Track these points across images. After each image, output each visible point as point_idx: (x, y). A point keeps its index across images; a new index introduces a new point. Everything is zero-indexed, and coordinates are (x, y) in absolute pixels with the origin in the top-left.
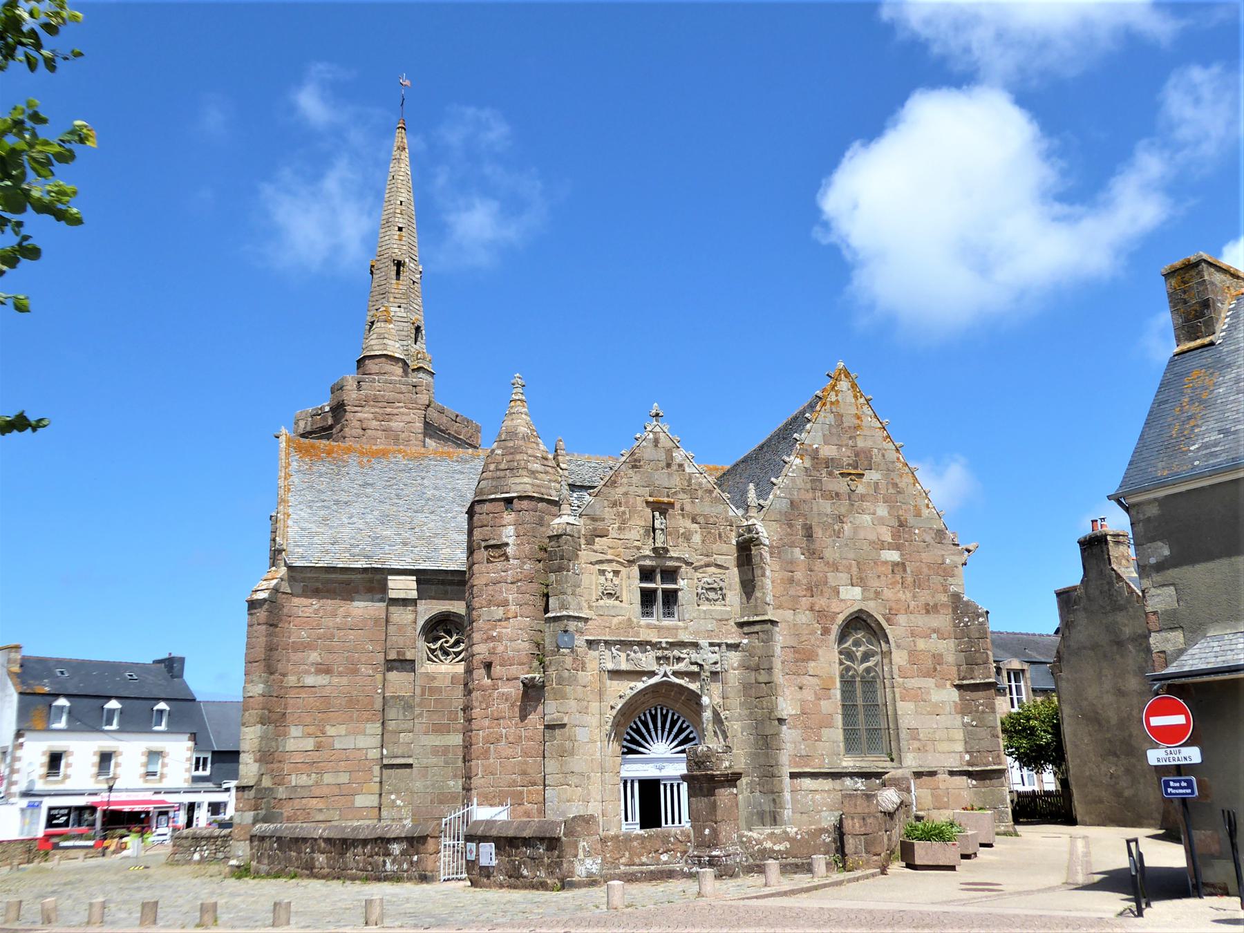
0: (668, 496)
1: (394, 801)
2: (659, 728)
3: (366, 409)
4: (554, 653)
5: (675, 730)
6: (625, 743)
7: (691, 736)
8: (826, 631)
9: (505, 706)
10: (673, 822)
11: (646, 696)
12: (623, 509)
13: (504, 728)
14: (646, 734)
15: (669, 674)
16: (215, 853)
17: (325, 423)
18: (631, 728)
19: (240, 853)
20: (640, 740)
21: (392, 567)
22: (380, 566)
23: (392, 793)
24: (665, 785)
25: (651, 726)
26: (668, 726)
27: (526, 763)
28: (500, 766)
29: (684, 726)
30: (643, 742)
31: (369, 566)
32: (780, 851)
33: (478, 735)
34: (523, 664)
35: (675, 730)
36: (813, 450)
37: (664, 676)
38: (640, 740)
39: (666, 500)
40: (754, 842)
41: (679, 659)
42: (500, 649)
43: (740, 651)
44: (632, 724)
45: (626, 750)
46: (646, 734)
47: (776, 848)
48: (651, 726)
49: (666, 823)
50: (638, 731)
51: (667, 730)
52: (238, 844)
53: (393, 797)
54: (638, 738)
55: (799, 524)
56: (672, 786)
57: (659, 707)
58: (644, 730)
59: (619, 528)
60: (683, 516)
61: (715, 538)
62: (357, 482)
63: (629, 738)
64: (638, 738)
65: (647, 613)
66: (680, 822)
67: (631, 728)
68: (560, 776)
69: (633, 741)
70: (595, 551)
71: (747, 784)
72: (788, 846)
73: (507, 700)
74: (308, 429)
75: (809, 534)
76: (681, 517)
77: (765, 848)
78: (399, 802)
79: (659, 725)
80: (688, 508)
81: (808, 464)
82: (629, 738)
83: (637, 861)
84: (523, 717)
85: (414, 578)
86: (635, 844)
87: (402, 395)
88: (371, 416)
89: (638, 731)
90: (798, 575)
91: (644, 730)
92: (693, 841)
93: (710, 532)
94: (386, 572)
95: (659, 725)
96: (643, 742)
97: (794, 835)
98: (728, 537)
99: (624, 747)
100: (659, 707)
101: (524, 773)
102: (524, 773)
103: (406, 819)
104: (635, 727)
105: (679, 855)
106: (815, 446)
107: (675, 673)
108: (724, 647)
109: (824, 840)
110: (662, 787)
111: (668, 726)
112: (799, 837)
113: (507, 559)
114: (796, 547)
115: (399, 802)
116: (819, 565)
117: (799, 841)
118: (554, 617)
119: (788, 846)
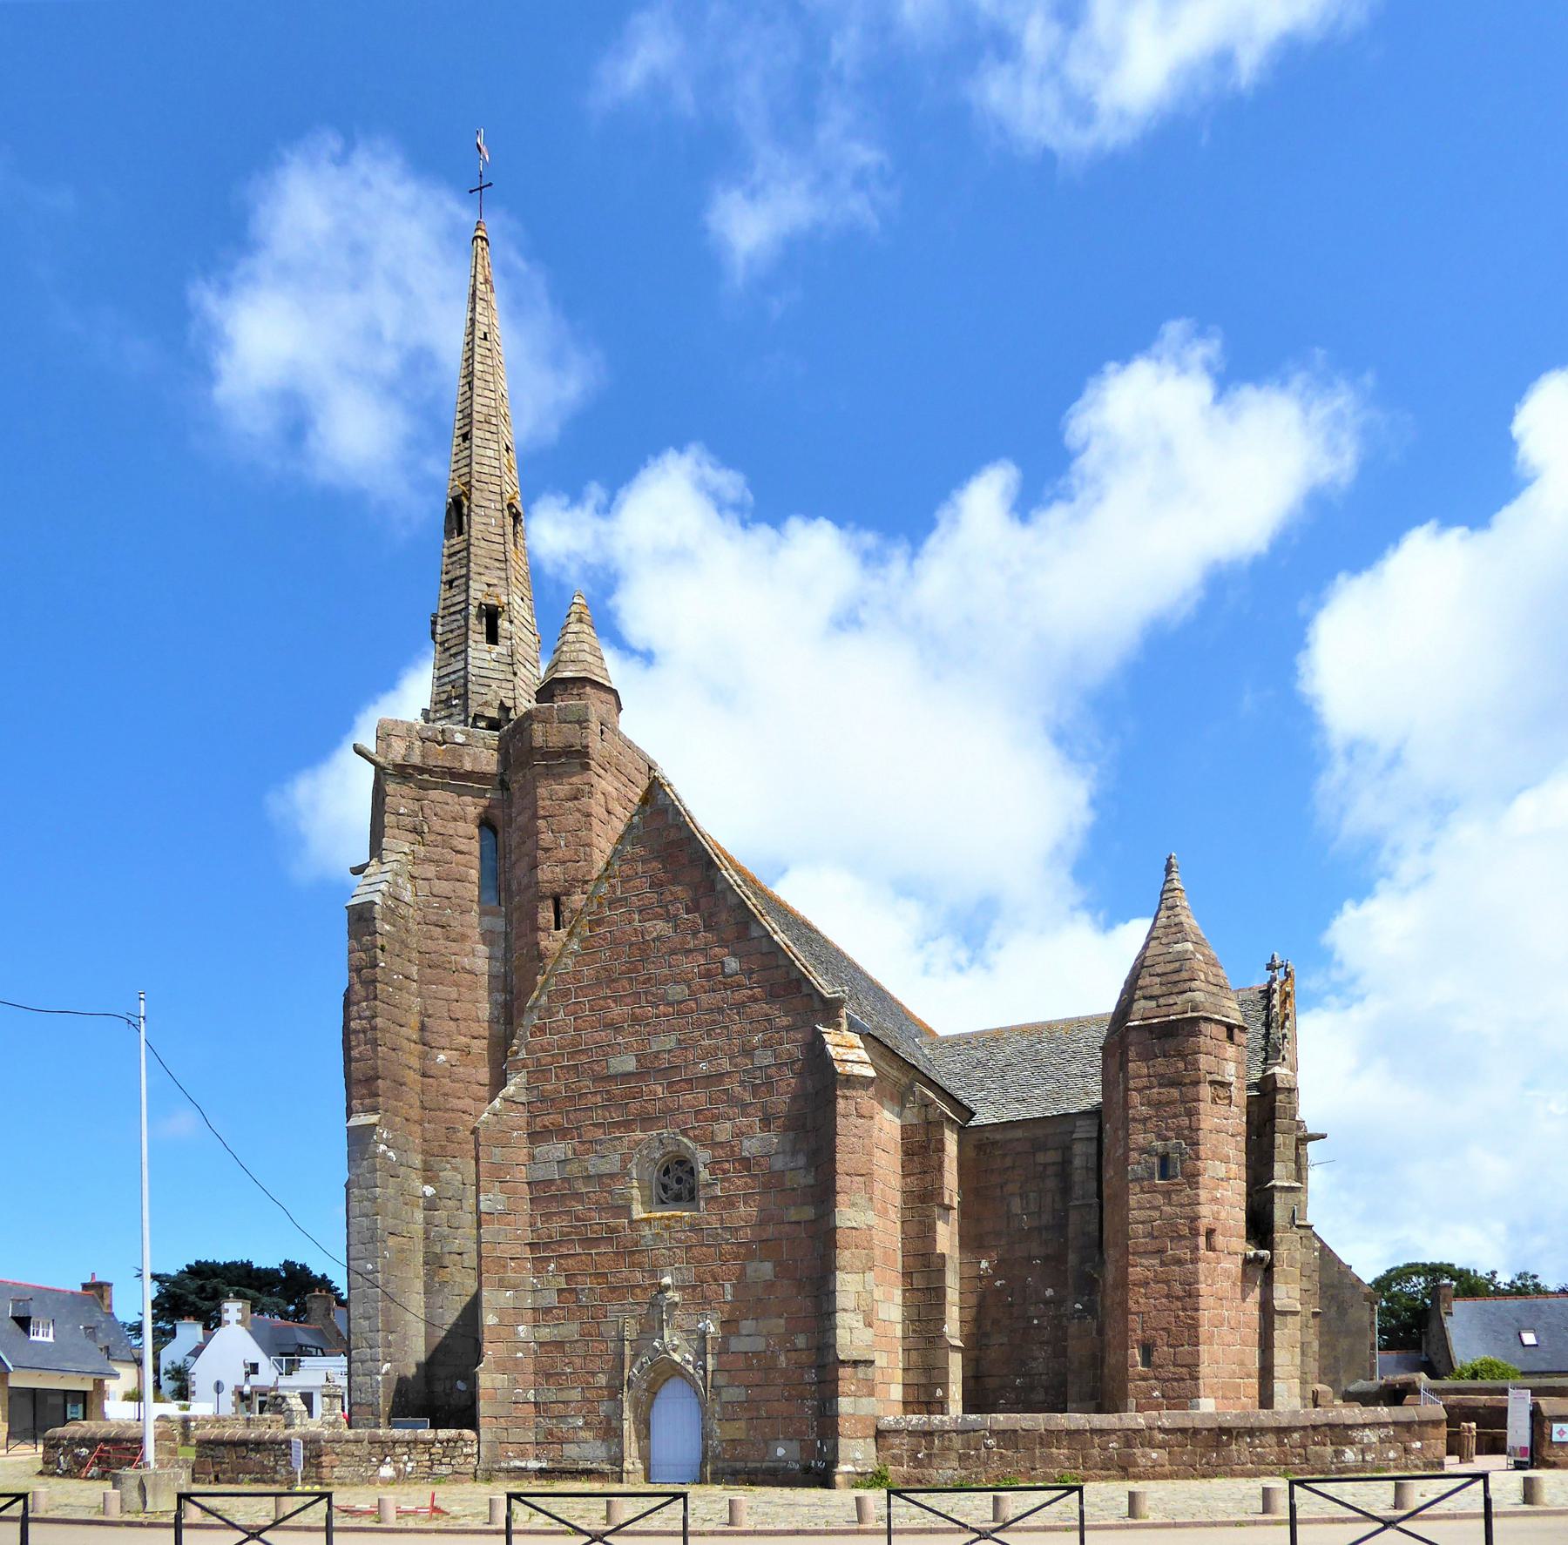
3: (609, 777)
4: (1285, 1230)
9: (1227, 1284)
16: (431, 1467)
17: (457, 765)
19: (858, 1455)
27: (1243, 1352)
33: (1204, 1315)
42: (1223, 1215)
52: (853, 1442)
68: (1291, 1368)
74: (416, 759)
84: (1244, 1300)
87: (639, 775)
88: (615, 793)
101: (1242, 1364)
118: (1288, 1187)
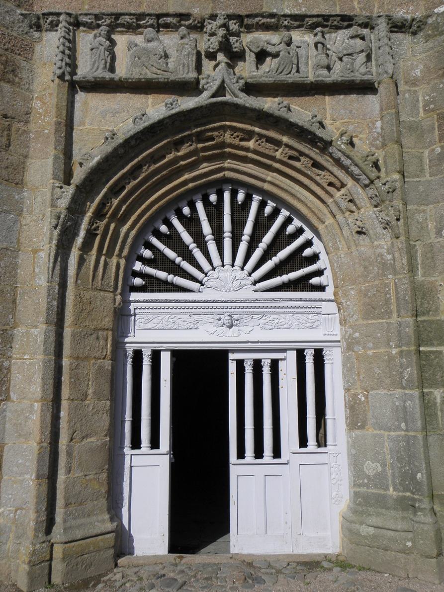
5: (268, 238)
10: (259, 453)
24: (240, 364)
25: (206, 228)
26: (248, 229)
30: (185, 265)
35: (268, 238)
37: (221, 90)
41: (261, 56)
43: (427, 38)
48: (206, 228)
49: (241, 454)
56: (257, 366)
58: (186, 238)
64: (171, 254)
66: (277, 453)
91: (186, 238)
96: (185, 265)
107: (251, 89)
108: (382, 27)
110: (232, 368)
111: (248, 229)
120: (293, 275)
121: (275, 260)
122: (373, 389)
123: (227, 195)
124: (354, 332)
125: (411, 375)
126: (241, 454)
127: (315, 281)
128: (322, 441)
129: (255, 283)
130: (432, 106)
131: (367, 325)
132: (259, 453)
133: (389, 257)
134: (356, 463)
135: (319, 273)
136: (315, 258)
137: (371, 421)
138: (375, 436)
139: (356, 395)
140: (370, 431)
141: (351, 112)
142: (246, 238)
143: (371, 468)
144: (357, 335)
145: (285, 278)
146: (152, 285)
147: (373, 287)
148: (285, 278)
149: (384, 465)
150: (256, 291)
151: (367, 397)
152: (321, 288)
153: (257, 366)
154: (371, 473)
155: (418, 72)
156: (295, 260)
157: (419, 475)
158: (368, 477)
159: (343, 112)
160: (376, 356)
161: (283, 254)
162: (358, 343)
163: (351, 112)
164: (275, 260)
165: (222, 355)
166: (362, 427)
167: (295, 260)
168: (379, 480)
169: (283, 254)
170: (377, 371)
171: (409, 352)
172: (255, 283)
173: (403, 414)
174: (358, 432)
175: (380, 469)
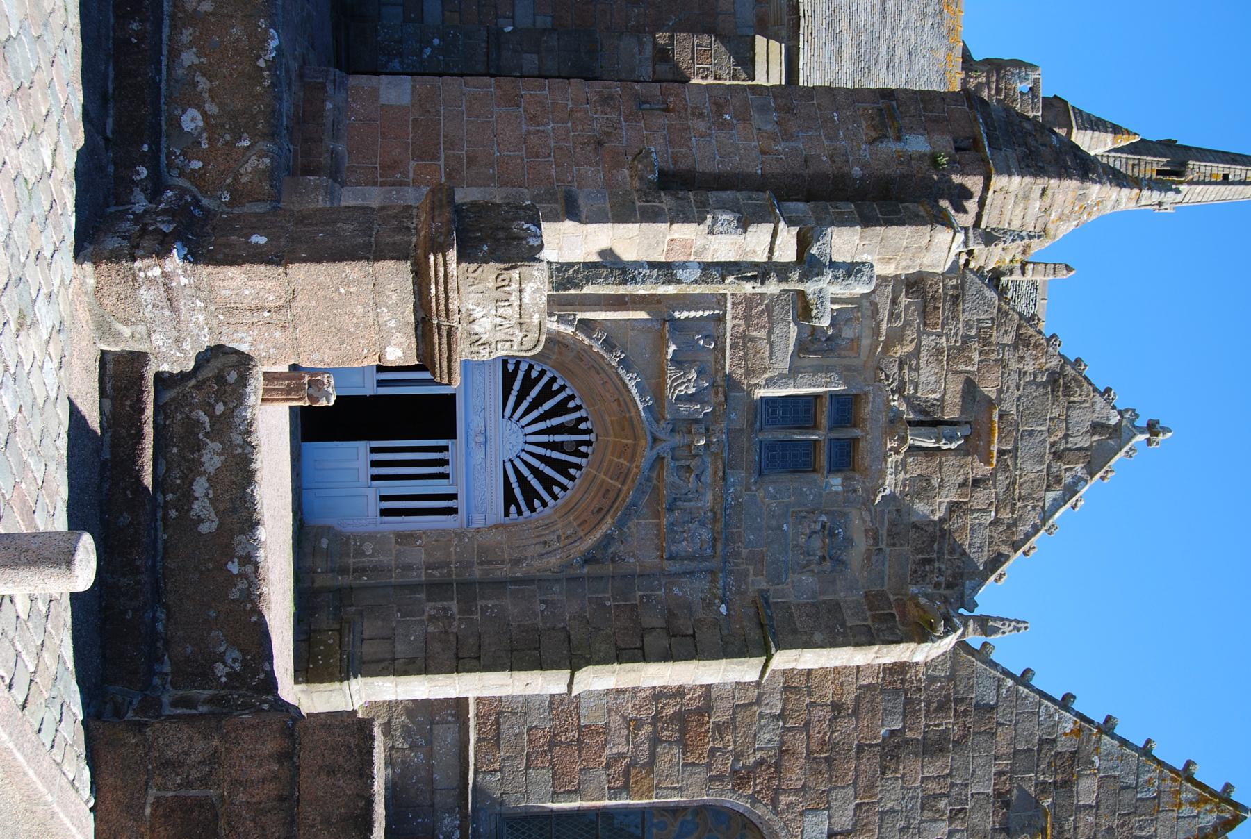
0: (1001, 453)
1: (430, 43)
2: (551, 438)
5: (548, 471)
6: (524, 367)
7: (537, 503)
8: (740, 779)
10: (375, 464)
11: (615, 405)
12: (976, 357)
13: (553, 129)
14: (541, 410)
15: (658, 448)
18: (553, 380)
20: (529, 399)
21: (801, 51)
22: (802, 31)
23: (442, 39)
25: (555, 421)
26: (555, 455)
28: (483, 123)
29: (556, 489)
31: (802, 14)
32: (188, 496)
34: (675, 163)
35: (548, 471)
36: (1088, 755)
38: (529, 399)
39: (995, 448)
40: (220, 408)
44: (560, 382)
45: (511, 368)
46: (541, 410)
47: (200, 486)
48: (555, 421)
49: (373, 450)
50: (546, 394)
51: (548, 453)
53: (436, 42)
54: (534, 393)
55: (948, 723)
57: (592, 437)
58: (547, 406)
59: (939, 351)
60: (963, 485)
61: (920, 551)
62: (913, 37)
63: (534, 374)
64: (534, 393)
65: (774, 412)
67: (553, 380)
69: (528, 383)
70: (894, 301)
71: (446, 610)
72: (205, 528)
73: (608, 134)
75: (933, 747)
76: (961, 479)
77: (199, 447)
78: (428, 51)
79: (558, 438)
80: (980, 498)
81: (1064, 746)
82: (534, 374)
83: (186, 35)
85: (783, 83)
86: (237, 31)
89: (546, 394)
90: (847, 725)
91: (547, 406)
92: (237, 211)
93: (933, 541)
94: (793, 43)
95: (558, 438)
97: (240, 551)
98: (924, 577)
99: (517, 364)
100: (592, 437)
102: (471, 160)
103: (401, 63)
104: (555, 387)
105: (196, 165)
106: (1096, 758)
109: (221, 658)
112: (234, 568)
113: (871, 142)
114: (904, 721)
115: (428, 51)
116: (870, 764)
117: (222, 568)
119: (205, 528)
120: (517, 492)
121: (530, 477)
122: (425, 550)
123: (585, 437)
124: (469, 538)
125: (434, 576)
126: (373, 450)
127: (513, 508)
128: (385, 512)
129: (511, 461)
130: (645, 601)
131: (473, 547)
132: (375, 464)
133: (524, 565)
134: (371, 537)
135: (520, 512)
136: (532, 509)
137: (402, 548)
138: (390, 550)
139: (421, 538)
140: (394, 547)
141: (643, 539)
142: (548, 453)
143: (368, 548)
144: (467, 540)
145: (515, 485)
146: (508, 379)
147: (502, 552)
148: (515, 485)
149: (370, 556)
150: (504, 462)
151: (418, 546)
152: (507, 514)
153: (444, 462)
154: (364, 547)
155: (677, 591)
156: (530, 494)
157: (366, 578)
158: (361, 545)
159: (643, 532)
160: (450, 553)
161: (535, 483)
162: (460, 540)
163: (643, 539)
164: (530, 477)
165: (452, 435)
166: (397, 542)
167: (530, 494)
168: (359, 553)
169: (535, 483)
170: (439, 553)
171: (451, 575)
172: (511, 461)
173: (407, 568)
174: (393, 541)
175: (368, 553)
